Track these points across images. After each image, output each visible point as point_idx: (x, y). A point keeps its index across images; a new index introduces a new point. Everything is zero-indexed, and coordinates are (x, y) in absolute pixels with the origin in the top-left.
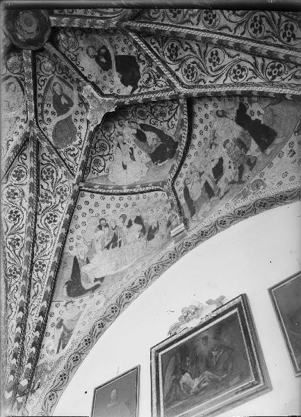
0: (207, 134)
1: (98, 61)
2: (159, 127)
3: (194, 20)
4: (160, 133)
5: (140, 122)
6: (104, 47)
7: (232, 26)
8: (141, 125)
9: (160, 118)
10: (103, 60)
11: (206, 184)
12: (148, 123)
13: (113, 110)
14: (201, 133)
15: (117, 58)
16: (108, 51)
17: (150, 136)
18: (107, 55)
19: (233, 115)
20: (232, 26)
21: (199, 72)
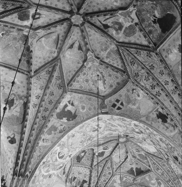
0: (81, 171)
1: (106, 147)
2: (84, 157)
3: (105, 172)
4: (83, 157)
5: (87, 152)
6: (108, 149)
7: (101, 180)
8: (86, 152)
9: (87, 158)
10: (106, 148)
11: (72, 177)
12: (86, 154)
13: (94, 152)
14: (81, 169)
15: (104, 152)
16: (107, 150)
17: (83, 154)
18: (106, 149)
19: (85, 179)
20: (101, 180)
21: (95, 172)
